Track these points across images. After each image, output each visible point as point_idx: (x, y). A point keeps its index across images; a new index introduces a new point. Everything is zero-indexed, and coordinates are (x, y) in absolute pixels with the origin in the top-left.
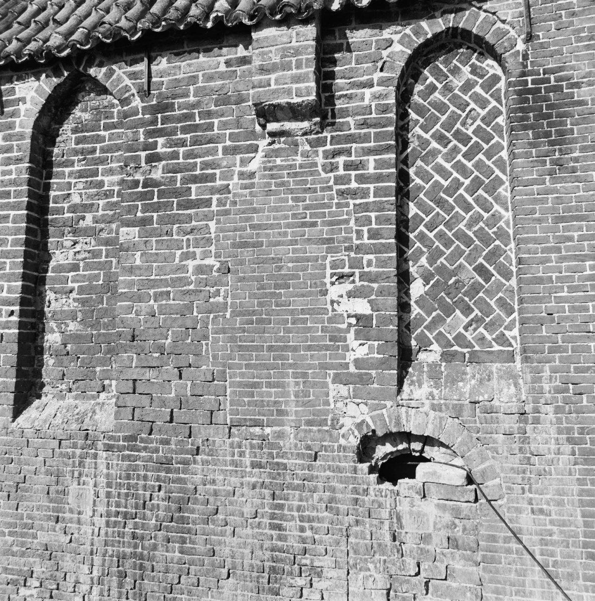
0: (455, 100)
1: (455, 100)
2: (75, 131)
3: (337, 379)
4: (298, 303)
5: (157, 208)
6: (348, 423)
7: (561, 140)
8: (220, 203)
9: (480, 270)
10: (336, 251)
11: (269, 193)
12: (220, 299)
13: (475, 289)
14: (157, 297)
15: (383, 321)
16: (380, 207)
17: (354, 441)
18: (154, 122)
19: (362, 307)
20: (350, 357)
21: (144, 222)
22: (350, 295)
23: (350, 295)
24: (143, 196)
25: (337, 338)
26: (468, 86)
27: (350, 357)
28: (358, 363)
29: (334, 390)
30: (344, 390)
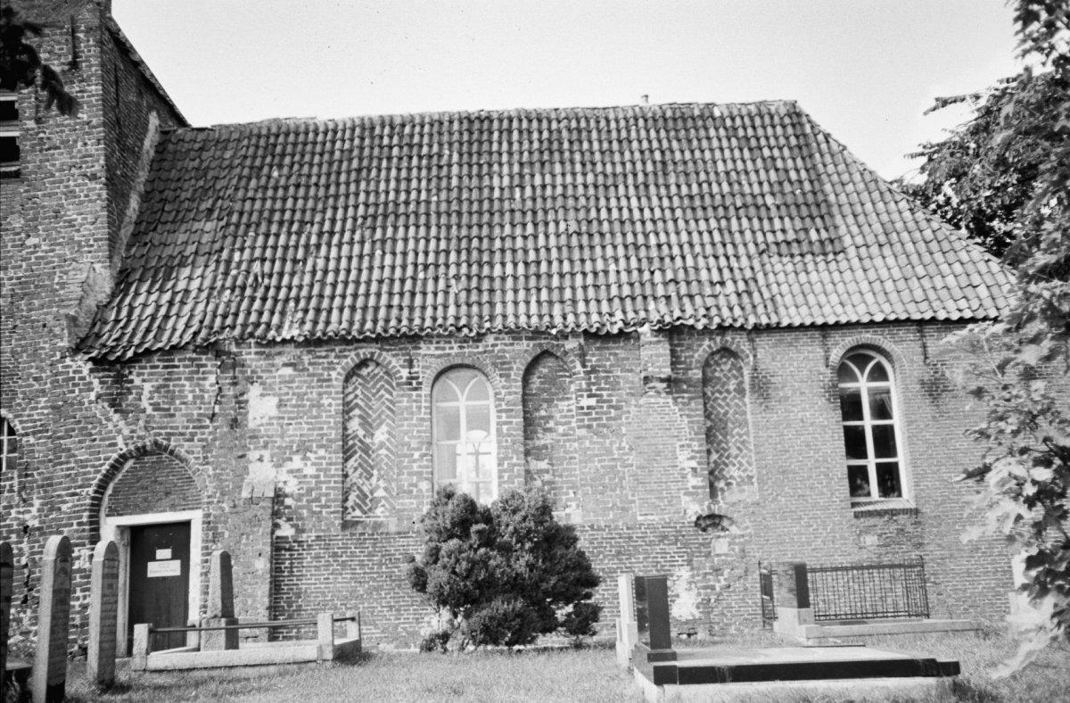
0: (725, 375)
1: (725, 375)
2: (540, 377)
3: (685, 494)
4: (666, 463)
5: (596, 419)
6: (690, 512)
7: (767, 398)
8: (627, 418)
9: (739, 448)
10: (681, 440)
11: (650, 415)
12: (630, 462)
13: (736, 457)
14: (600, 461)
15: (702, 469)
16: (698, 422)
17: (694, 519)
18: (590, 379)
19: (694, 464)
20: (689, 485)
21: (589, 427)
22: (688, 459)
23: (688, 459)
24: (586, 414)
25: (684, 477)
26: (730, 370)
27: (689, 485)
28: (694, 487)
29: (685, 499)
30: (688, 499)
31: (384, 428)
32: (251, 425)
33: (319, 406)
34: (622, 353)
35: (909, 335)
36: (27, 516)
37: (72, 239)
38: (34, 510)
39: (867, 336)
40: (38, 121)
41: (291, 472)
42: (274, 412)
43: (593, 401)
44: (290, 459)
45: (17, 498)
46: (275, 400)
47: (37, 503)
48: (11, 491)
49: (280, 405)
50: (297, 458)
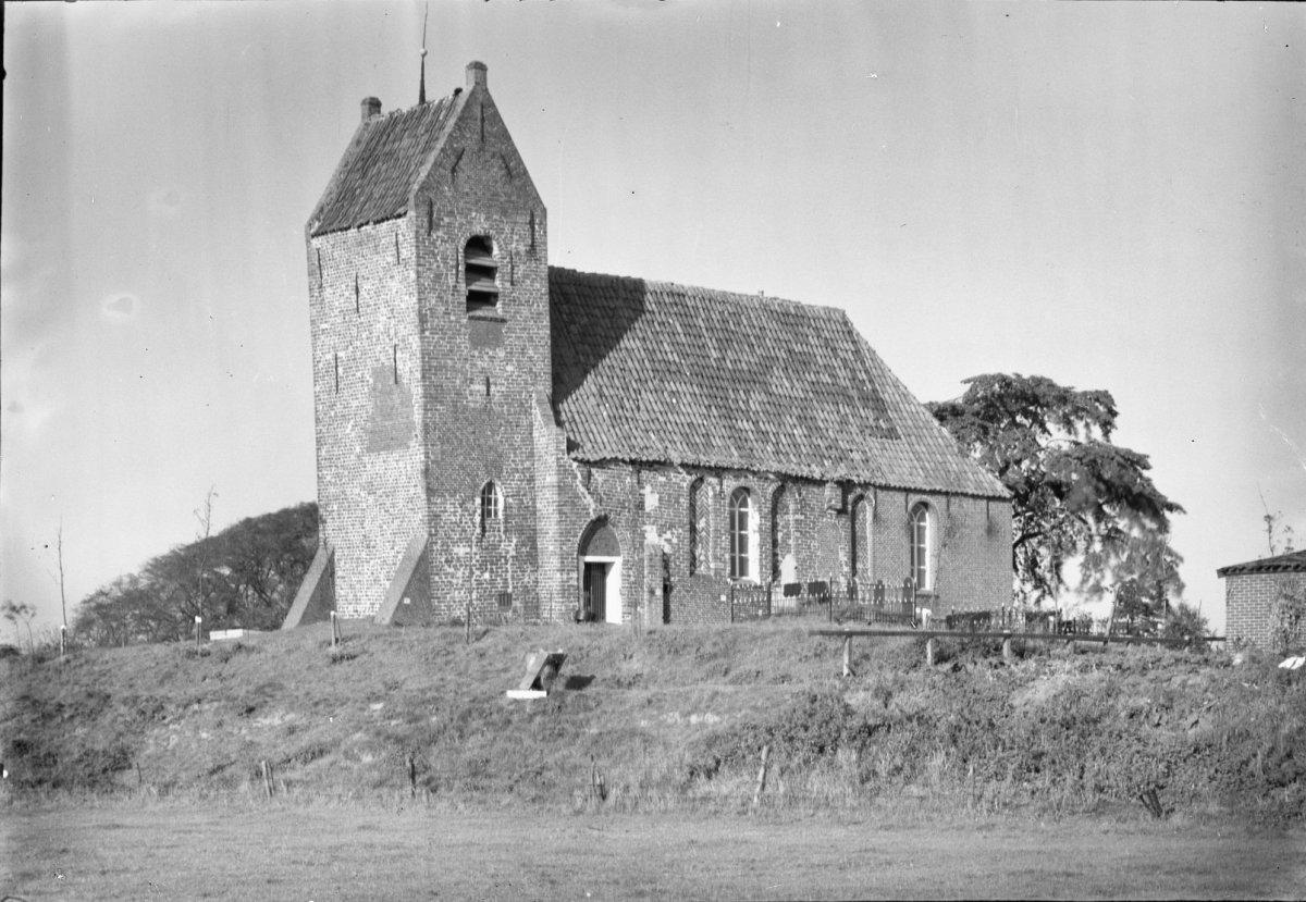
31: (704, 519)
32: (647, 510)
33: (679, 503)
34: (815, 490)
35: (943, 499)
36: (510, 548)
37: (531, 369)
38: (513, 545)
39: (925, 498)
40: (512, 284)
41: (666, 540)
42: (657, 504)
43: (803, 517)
44: (665, 533)
45: (503, 537)
46: (657, 496)
47: (515, 541)
48: (499, 531)
49: (660, 500)
50: (669, 532)
